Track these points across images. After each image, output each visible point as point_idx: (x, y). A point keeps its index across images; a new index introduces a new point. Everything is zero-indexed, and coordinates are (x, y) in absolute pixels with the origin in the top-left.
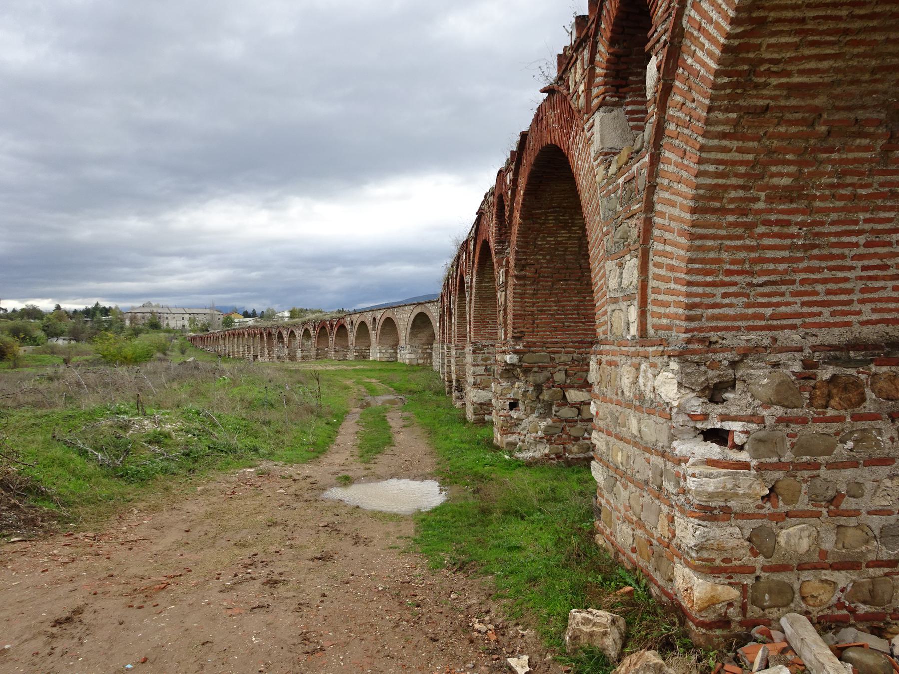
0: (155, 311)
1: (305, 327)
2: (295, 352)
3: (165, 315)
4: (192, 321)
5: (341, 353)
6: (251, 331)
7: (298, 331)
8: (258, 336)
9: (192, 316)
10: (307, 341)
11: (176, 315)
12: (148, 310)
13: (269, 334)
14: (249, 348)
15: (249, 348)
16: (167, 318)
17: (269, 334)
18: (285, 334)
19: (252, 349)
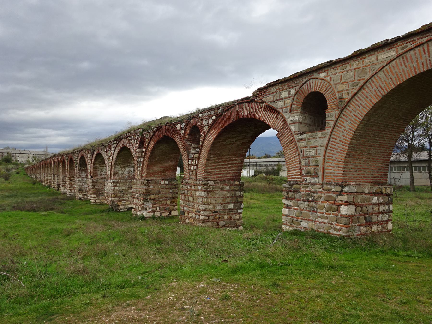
0: (10, 152)
1: (121, 145)
2: (103, 184)
3: (17, 155)
4: (34, 159)
5: (219, 193)
6: (56, 159)
7: (109, 153)
8: (61, 164)
9: (34, 156)
10: (123, 168)
11: (24, 155)
12: (6, 151)
13: (71, 161)
14: (54, 176)
15: (54, 176)
16: (18, 157)
17: (71, 161)
18: (89, 160)
19: (56, 178)
